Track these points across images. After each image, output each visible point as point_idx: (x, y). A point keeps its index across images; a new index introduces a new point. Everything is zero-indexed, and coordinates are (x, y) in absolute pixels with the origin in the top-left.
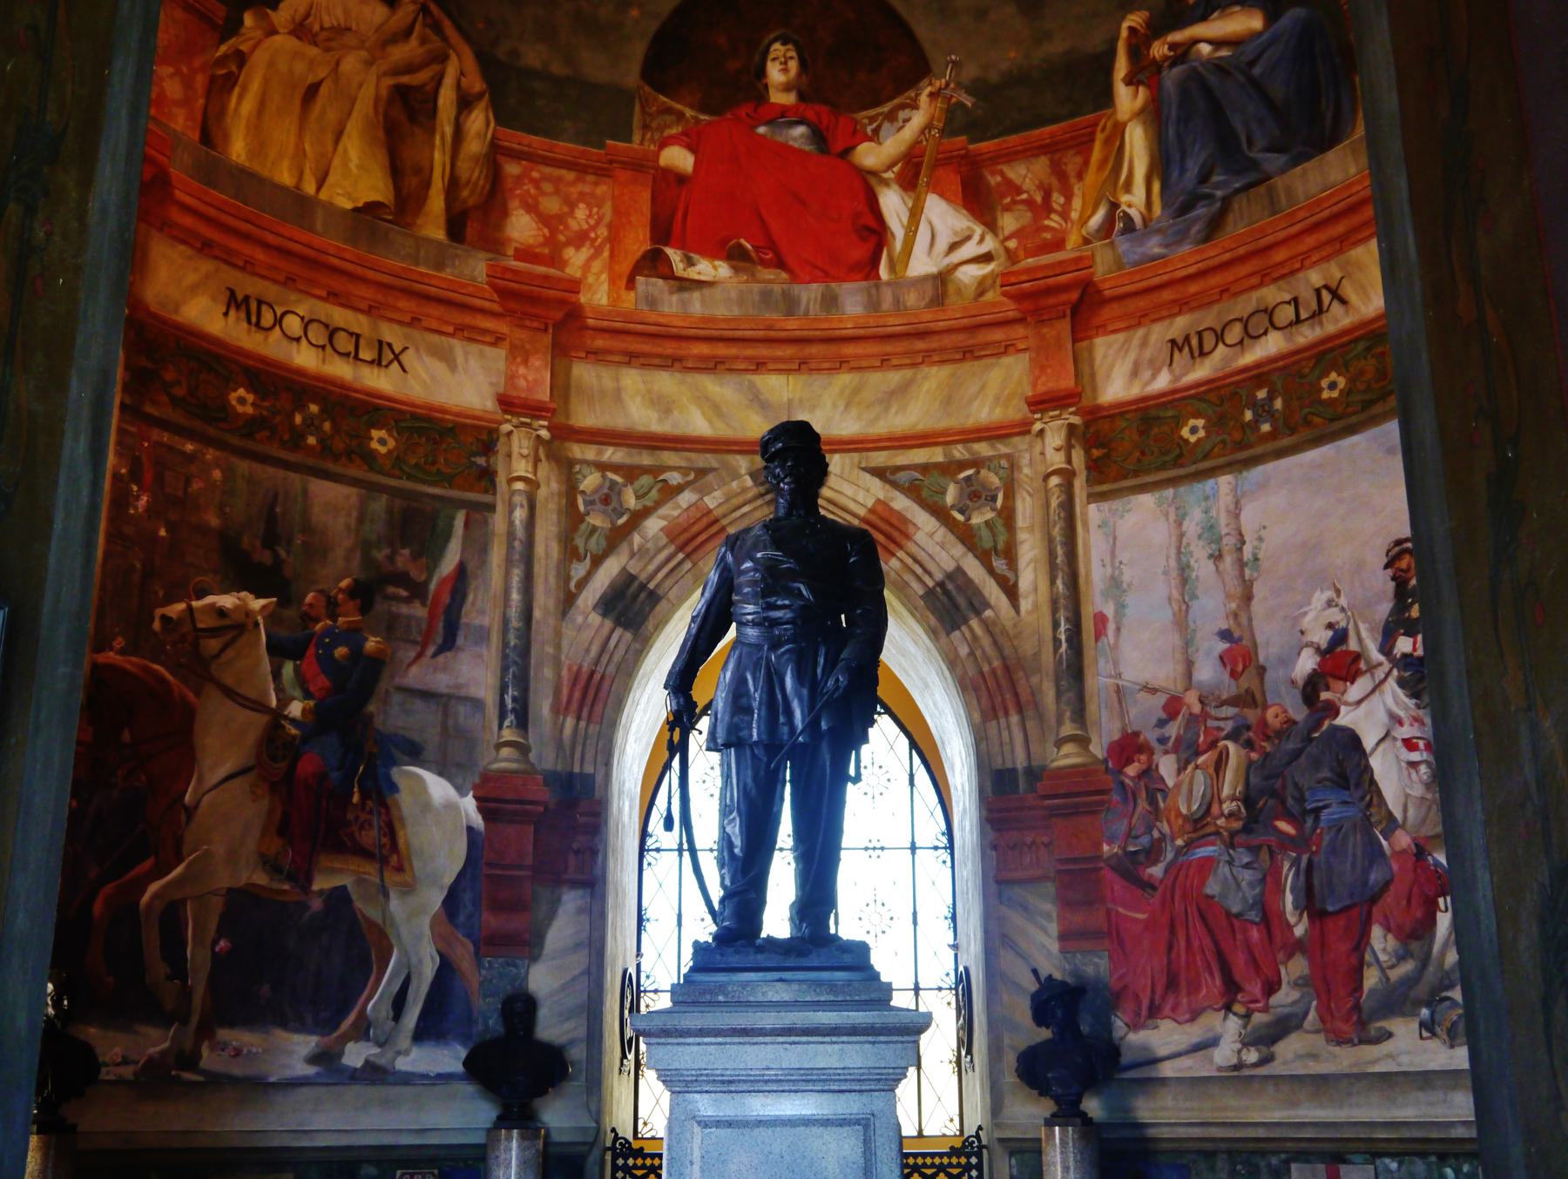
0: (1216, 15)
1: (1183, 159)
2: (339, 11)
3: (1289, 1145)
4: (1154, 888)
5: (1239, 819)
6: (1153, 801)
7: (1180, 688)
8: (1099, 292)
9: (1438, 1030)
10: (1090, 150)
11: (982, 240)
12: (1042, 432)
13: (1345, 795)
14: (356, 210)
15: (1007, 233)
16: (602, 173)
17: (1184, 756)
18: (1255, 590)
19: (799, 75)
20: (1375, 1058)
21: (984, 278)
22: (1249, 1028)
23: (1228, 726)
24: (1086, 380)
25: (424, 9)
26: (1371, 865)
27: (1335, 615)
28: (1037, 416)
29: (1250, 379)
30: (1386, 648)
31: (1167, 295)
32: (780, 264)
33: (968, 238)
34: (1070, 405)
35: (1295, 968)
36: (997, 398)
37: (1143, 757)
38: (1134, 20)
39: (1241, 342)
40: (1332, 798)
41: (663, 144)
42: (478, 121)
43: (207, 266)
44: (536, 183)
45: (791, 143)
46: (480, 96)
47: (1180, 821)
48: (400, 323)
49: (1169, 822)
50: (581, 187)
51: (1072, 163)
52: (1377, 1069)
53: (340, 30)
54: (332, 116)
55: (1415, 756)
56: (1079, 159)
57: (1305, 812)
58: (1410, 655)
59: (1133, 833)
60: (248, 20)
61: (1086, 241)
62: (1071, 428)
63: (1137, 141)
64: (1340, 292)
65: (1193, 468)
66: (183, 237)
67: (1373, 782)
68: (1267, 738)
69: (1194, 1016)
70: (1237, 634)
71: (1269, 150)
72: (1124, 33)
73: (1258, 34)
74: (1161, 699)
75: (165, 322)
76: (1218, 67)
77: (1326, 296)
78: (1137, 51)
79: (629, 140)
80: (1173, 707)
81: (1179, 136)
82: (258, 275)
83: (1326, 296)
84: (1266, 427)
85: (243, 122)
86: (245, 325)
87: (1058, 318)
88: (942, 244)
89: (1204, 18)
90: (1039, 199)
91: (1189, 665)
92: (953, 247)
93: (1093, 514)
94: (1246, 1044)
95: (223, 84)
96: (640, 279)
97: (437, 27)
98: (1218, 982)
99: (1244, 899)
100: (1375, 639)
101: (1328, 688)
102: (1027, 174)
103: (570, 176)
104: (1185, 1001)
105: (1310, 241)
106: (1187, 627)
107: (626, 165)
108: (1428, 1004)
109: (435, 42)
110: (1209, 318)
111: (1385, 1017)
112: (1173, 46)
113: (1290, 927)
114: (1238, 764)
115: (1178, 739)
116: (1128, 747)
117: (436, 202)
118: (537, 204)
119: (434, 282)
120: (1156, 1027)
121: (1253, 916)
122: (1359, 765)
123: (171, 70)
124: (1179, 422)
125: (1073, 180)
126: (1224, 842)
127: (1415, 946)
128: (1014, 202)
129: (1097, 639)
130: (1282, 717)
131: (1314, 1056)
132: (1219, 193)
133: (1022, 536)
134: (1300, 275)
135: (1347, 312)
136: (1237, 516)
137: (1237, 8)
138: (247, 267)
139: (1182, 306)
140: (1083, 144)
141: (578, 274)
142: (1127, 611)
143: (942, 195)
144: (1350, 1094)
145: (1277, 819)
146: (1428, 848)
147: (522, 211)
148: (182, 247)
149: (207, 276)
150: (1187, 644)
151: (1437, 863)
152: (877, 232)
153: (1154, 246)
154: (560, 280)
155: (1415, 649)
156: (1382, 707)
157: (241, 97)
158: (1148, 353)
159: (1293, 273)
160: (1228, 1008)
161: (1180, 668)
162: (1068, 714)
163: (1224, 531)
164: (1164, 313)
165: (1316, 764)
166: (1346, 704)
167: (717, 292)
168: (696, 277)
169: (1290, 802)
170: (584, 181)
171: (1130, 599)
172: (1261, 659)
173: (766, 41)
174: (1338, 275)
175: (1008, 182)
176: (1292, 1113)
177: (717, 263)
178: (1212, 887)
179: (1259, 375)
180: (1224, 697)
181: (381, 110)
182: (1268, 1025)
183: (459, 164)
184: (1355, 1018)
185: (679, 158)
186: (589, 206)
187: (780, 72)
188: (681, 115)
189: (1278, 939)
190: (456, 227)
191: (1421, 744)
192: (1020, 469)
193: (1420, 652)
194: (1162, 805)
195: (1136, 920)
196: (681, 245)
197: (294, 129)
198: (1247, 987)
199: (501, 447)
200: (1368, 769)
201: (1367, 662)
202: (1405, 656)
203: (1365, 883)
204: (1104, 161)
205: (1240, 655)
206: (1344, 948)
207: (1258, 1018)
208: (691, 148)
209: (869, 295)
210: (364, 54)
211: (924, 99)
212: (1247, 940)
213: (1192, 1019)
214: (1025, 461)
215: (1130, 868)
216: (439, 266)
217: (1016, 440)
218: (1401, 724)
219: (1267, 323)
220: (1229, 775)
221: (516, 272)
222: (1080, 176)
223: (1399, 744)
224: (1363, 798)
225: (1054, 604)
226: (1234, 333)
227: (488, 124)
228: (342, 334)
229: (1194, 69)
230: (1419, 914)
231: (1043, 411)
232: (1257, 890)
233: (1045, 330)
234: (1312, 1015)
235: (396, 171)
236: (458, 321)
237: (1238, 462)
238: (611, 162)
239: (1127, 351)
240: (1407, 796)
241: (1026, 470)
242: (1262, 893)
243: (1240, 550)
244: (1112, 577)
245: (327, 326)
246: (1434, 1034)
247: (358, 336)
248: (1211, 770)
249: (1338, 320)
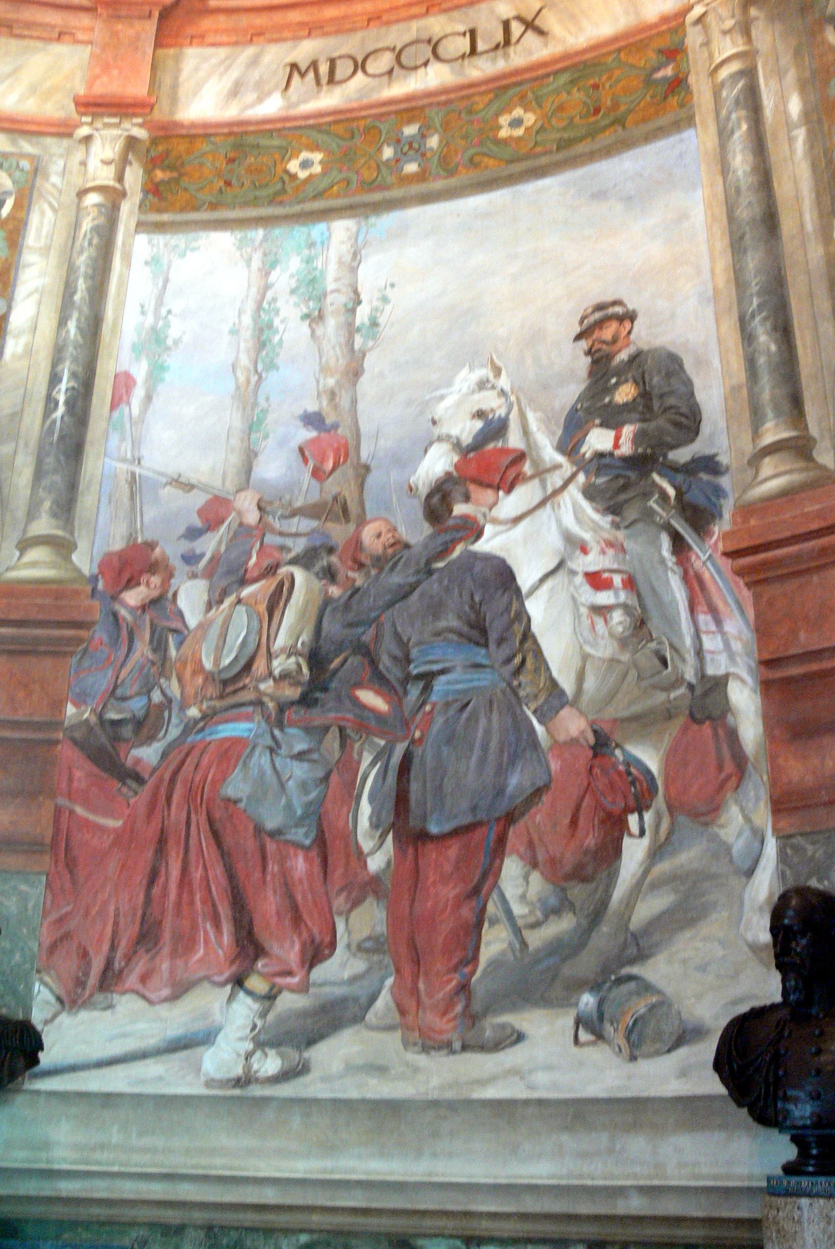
3: (315, 1218)
4: (139, 779)
5: (298, 683)
6: (159, 646)
7: (230, 486)
9: (609, 1029)
12: (88, 139)
13: (480, 655)
17: (223, 583)
18: (366, 365)
20: (489, 1075)
22: (271, 1017)
23: (299, 546)
24: (165, 90)
26: (512, 762)
27: (490, 401)
28: (87, 119)
29: (396, 112)
30: (569, 445)
34: (135, 115)
35: (369, 919)
36: (33, 89)
37: (155, 580)
39: (390, 72)
40: (456, 657)
47: (200, 680)
49: (180, 680)
52: (491, 1093)
55: (604, 598)
57: (408, 678)
58: (611, 454)
59: (119, 692)
62: (131, 143)
65: (297, 208)
67: (527, 635)
68: (361, 566)
69: (179, 990)
70: (329, 421)
74: (199, 499)
80: (214, 513)
83: (516, 28)
84: (411, 168)
87: (141, 18)
91: (250, 457)
93: (141, 252)
94: (262, 1042)
98: (227, 938)
99: (289, 806)
100: (551, 433)
101: (467, 499)
104: (165, 966)
106: (255, 404)
108: (595, 987)
110: (350, 45)
111: (513, 1008)
113: (361, 857)
114: (307, 603)
115: (215, 560)
116: (133, 564)
120: (110, 1007)
121: (302, 835)
122: (508, 609)
124: (286, 153)
126: (268, 719)
127: (577, 892)
129: (113, 406)
130: (387, 538)
131: (380, 1070)
133: (28, 257)
136: (354, 270)
142: (167, 376)
144: (435, 1134)
145: (359, 685)
146: (617, 737)
150: (253, 425)
151: (631, 762)
155: (616, 446)
156: (554, 527)
158: (256, 74)
160: (239, 982)
161: (235, 459)
162: (47, 505)
163: (330, 286)
165: (436, 609)
166: (495, 521)
169: (385, 662)
171: (172, 361)
172: (364, 455)
176: (329, 1163)
178: (236, 786)
179: (411, 108)
180: (299, 503)
182: (304, 1014)
184: (459, 1008)
189: (337, 874)
191: (617, 580)
192: (46, 177)
193: (626, 449)
194: (173, 652)
195: (103, 829)
198: (275, 948)
200: (522, 616)
201: (535, 463)
202: (600, 455)
203: (500, 792)
205: (331, 446)
206: (450, 892)
207: (288, 1002)
212: (285, 874)
213: (174, 997)
214: (57, 166)
215: (105, 751)
217: (49, 141)
218: (584, 550)
219: (429, 54)
220: (290, 616)
223: (579, 579)
224: (509, 660)
225: (58, 353)
230: (591, 841)
231: (94, 116)
232: (313, 795)
233: (119, 27)
234: (384, 1001)
237: (365, 205)
239: (228, 68)
240: (585, 657)
241: (55, 179)
242: (321, 802)
243: (353, 311)
244: (154, 329)
246: (600, 1036)
248: (263, 608)
249: (529, 51)
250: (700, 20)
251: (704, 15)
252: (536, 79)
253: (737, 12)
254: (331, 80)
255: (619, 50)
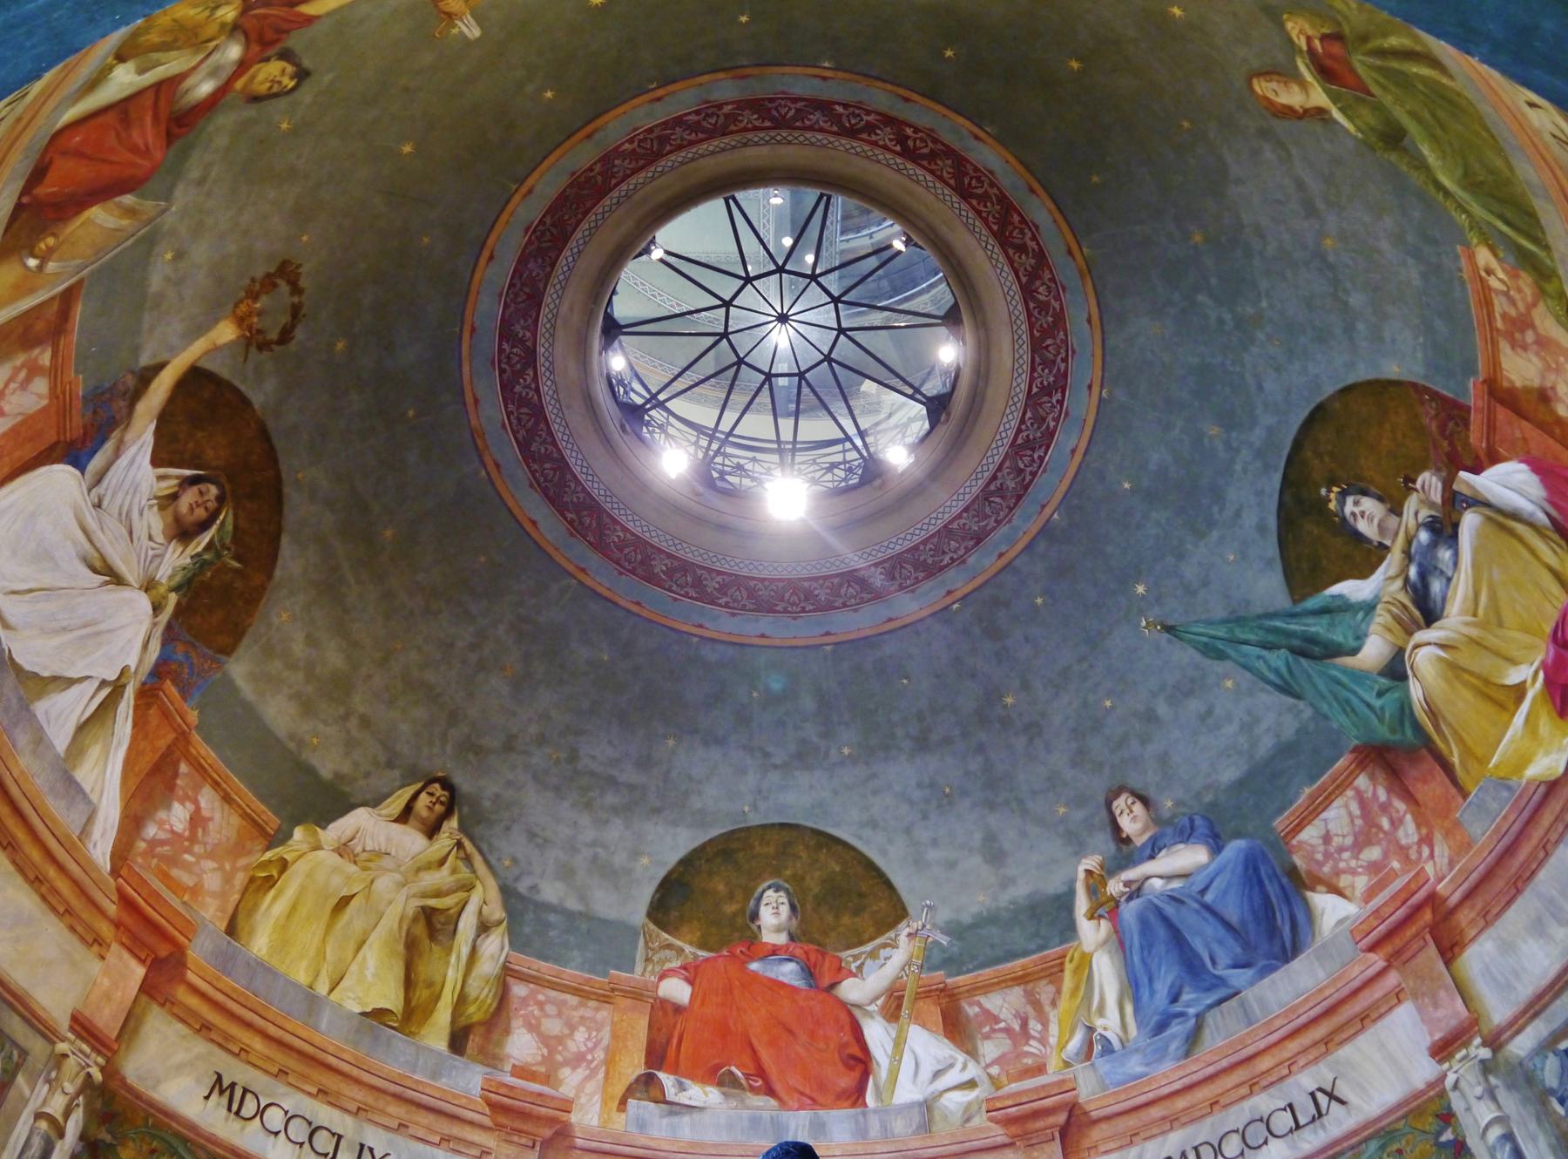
0: (1163, 852)
1: (1151, 980)
2: (382, 840)
8: (1086, 1113)
10: (1061, 980)
11: (964, 1067)
14: (364, 1014)
15: (988, 1061)
16: (604, 999)
19: (790, 918)
21: (970, 1104)
25: (459, 845)
31: (1155, 1112)
32: (770, 1091)
33: (951, 1066)
38: (1091, 862)
41: (662, 977)
42: (494, 947)
43: (200, 1046)
44: (541, 1005)
45: (781, 978)
46: (500, 923)
48: (386, 1128)
50: (581, 1012)
51: (1045, 991)
53: (381, 854)
54: (358, 925)
56: (1051, 989)
60: (298, 833)
61: (1067, 1064)
63: (1106, 973)
64: (1336, 1093)
66: (183, 1016)
71: (1235, 966)
72: (1081, 875)
73: (1205, 867)
75: (138, 1095)
76: (1173, 899)
77: (1323, 1099)
78: (1092, 891)
79: (632, 971)
81: (1143, 961)
82: (249, 1063)
83: (1323, 1099)
85: (272, 921)
86: (224, 1111)
88: (926, 1072)
89: (1152, 857)
90: (1016, 1027)
92: (937, 1074)
95: (262, 884)
96: (631, 1102)
97: (468, 859)
102: (1004, 1004)
103: (573, 1000)
105: (1293, 1046)
107: (627, 994)
109: (465, 873)
112: (1127, 884)
117: (443, 1016)
118: (539, 1024)
119: (428, 1091)
123: (215, 865)
125: (1047, 1008)
128: (994, 1031)
132: (1192, 1011)
134: (1290, 1080)
135: (1349, 1113)
137: (1181, 846)
138: (242, 1054)
139: (1172, 1122)
140: (1053, 972)
141: (571, 1095)
143: (923, 1026)
147: (523, 1030)
148: (180, 1026)
149: (197, 1058)
152: (861, 1062)
153: (1135, 1065)
154: (553, 1098)
157: (275, 898)
159: (1282, 1079)
164: (1155, 1131)
167: (706, 1117)
168: (687, 1102)
170: (585, 1006)
173: (760, 889)
174: (1330, 1078)
175: (987, 1012)
177: (709, 1089)
181: (405, 927)
183: (470, 981)
185: (677, 990)
186: (588, 1028)
187: (773, 915)
188: (680, 951)
190: (458, 1042)
196: (674, 1070)
197: (320, 933)
204: (1076, 989)
208: (690, 982)
209: (857, 1122)
210: (398, 877)
211: (903, 938)
216: (435, 1075)
221: (511, 1088)
222: (1054, 1004)
227: (502, 949)
228: (324, 1132)
229: (1150, 901)
235: (409, 983)
236: (446, 1131)
238: (613, 990)
245: (310, 1123)
247: (340, 1137)
250: (1456, 1086)
251: (1457, 1081)
252: (1352, 1148)
253: (1481, 1079)
255: (1405, 1116)
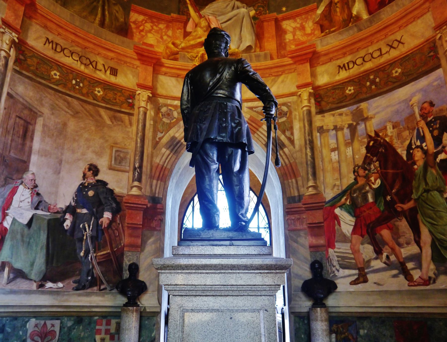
199: (137, 97)
226: (359, 61)
254: (349, 69)
